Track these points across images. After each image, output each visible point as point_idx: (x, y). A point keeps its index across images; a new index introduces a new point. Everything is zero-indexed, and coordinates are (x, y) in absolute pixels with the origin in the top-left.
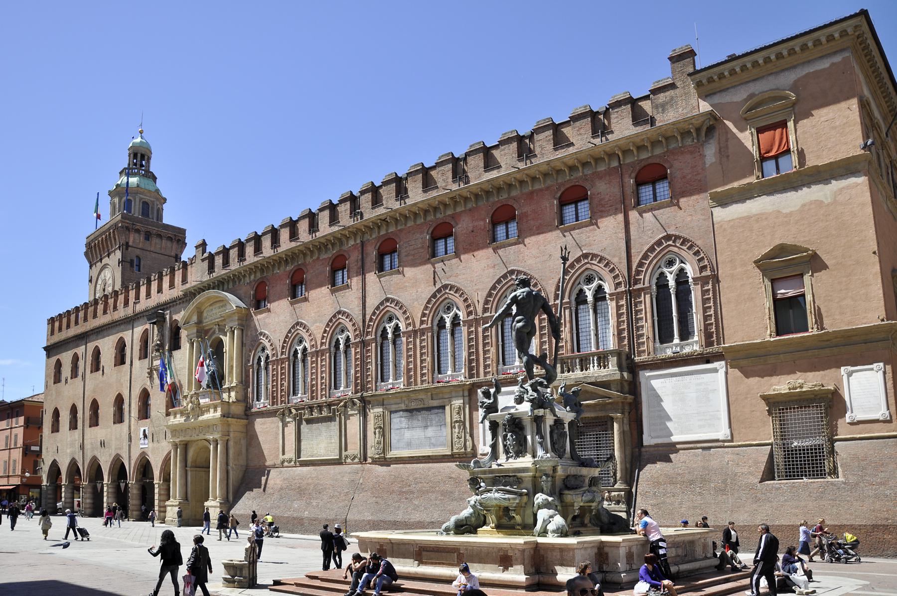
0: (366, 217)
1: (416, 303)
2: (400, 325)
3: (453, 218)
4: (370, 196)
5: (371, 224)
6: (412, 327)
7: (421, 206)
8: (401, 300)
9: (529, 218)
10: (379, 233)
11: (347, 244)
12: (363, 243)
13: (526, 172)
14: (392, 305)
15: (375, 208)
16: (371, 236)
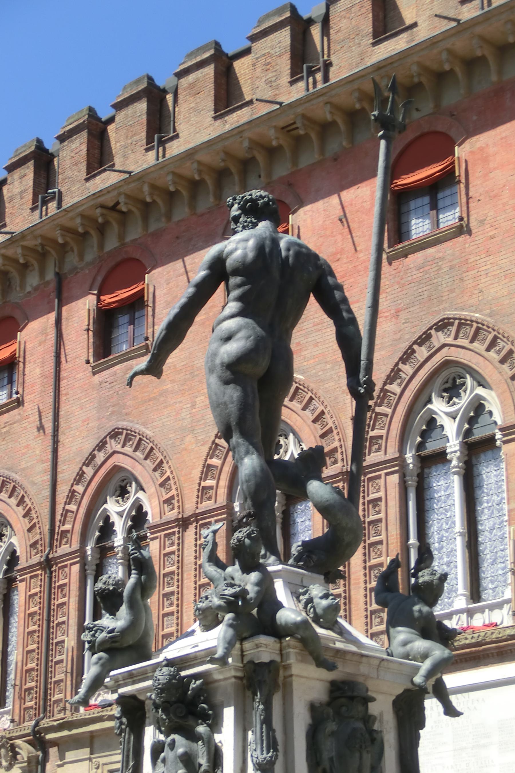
0: (68, 202)
1: (189, 439)
2: (147, 508)
3: (290, 185)
4: (84, 147)
5: (78, 220)
6: (176, 511)
7: (204, 157)
8: (149, 433)
9: (491, 165)
10: (101, 246)
11: (23, 286)
12: (60, 278)
13: (478, 30)
14: (128, 450)
15: (94, 176)
16: (81, 257)
